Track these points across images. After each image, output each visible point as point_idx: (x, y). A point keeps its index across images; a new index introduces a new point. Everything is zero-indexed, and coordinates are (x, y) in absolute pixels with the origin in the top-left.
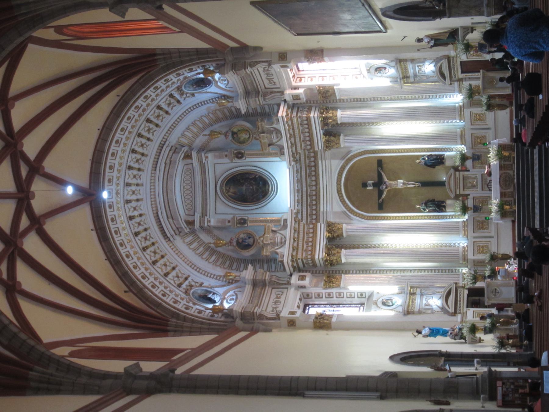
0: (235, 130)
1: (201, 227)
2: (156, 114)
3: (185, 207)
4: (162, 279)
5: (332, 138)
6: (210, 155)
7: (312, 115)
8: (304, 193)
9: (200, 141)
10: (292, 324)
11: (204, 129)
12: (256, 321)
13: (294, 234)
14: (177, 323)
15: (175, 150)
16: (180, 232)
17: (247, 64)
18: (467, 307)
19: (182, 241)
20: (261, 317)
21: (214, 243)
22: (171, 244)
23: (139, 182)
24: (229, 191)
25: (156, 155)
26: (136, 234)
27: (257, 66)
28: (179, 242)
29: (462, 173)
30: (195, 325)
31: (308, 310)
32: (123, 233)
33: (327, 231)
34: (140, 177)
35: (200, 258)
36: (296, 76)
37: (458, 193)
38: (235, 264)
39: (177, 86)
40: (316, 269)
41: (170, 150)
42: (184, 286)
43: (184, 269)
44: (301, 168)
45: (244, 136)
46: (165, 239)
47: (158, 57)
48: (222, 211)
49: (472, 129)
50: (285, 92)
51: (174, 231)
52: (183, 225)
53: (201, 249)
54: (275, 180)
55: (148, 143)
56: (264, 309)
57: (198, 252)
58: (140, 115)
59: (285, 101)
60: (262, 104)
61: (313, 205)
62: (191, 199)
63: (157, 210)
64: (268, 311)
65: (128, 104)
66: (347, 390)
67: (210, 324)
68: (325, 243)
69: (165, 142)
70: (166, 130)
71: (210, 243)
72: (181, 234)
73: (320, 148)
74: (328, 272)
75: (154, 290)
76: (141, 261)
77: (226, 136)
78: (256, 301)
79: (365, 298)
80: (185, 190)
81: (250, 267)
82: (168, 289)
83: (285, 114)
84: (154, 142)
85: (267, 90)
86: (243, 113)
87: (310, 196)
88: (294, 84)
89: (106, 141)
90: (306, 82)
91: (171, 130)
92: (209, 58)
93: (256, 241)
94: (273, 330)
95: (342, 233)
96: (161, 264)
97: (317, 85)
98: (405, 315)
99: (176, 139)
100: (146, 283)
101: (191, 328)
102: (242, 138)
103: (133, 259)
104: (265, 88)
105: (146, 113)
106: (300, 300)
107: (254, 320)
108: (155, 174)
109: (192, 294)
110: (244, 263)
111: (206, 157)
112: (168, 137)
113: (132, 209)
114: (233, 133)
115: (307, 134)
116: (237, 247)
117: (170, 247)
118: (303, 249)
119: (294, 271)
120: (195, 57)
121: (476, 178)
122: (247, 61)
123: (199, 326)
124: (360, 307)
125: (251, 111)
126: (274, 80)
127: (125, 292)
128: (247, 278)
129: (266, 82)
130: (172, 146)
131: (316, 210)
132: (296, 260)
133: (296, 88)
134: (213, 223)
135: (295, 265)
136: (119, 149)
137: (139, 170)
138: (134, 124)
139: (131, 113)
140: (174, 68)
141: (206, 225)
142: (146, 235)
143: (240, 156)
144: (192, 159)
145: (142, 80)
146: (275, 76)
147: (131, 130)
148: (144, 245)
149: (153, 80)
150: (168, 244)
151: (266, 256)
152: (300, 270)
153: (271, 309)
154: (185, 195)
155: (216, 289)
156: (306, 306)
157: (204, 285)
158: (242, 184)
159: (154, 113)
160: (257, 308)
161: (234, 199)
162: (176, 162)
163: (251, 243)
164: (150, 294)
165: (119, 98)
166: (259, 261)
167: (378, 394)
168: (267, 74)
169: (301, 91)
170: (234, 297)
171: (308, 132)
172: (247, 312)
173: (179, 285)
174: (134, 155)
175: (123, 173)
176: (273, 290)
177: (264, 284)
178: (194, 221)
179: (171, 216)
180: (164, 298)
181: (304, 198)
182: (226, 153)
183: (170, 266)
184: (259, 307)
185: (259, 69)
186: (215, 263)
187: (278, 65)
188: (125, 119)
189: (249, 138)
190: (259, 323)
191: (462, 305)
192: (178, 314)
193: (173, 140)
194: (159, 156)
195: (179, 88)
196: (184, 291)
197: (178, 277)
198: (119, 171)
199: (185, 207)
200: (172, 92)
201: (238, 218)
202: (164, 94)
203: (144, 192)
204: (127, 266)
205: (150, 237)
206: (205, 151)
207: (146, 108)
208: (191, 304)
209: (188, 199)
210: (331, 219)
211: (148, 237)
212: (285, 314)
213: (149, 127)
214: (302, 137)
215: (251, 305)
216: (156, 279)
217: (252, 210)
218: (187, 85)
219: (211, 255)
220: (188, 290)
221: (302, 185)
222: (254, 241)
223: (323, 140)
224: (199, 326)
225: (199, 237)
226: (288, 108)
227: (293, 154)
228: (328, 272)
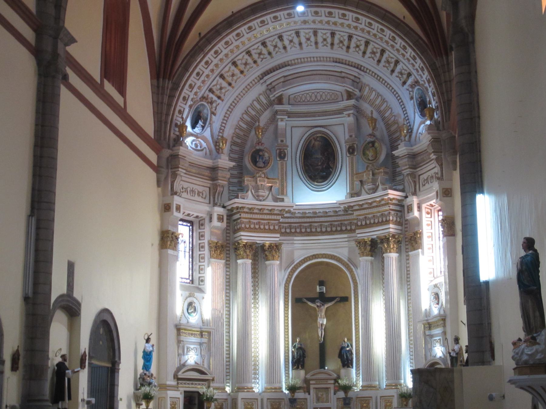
0: (376, 145)
1: (276, 113)
2: (390, 59)
3: (298, 94)
4: (217, 72)
5: (368, 248)
6: (351, 119)
7: (391, 226)
8: (313, 220)
9: (367, 108)
10: (167, 208)
11: (379, 112)
12: (170, 171)
13: (267, 209)
14: (168, 88)
15: (356, 82)
16: (270, 90)
17: (440, 154)
18: (185, 392)
19: (261, 92)
20: (175, 176)
21: (259, 125)
22: (256, 81)
23: (320, 45)
24: (315, 140)
25: (349, 62)
26: (264, 44)
27: (437, 165)
28: (260, 88)
29: (332, 386)
30: (165, 107)
31: (187, 225)
32: (264, 29)
34: (325, 45)
35: (244, 111)
36: (432, 208)
37: (311, 382)
38: (237, 149)
39: (420, 81)
40: (231, 233)
41: (355, 77)
42: (211, 95)
43: (230, 96)
44: (340, 215)
45: (370, 154)
46: (261, 74)
47: (444, 58)
48: (295, 134)
49: (377, 397)
50: (414, 197)
51: (271, 84)
52: (277, 93)
53: (253, 113)
54: (327, 189)
55: (361, 53)
56: (183, 179)
57: (250, 109)
58: (387, 42)
59: (406, 197)
60: (403, 172)
61: (301, 229)
62: (301, 101)
63: (292, 65)
64: (182, 183)
65: (396, 28)
66: (37, 261)
67: (166, 123)
68: (258, 242)
69: (363, 71)
70: (376, 71)
71: (259, 122)
72: (268, 92)
73: (359, 235)
74: (228, 245)
75: (203, 63)
76: (235, 49)
77: (370, 135)
78: (194, 171)
79: (199, 285)
80: (316, 93)
81: (232, 164)
82: (206, 79)
83: (391, 197)
84: (362, 59)
85: (417, 177)
86: (393, 152)
87: (311, 225)
88: (424, 206)
89: (357, 7)
90: (426, 220)
91: (376, 76)
92: (445, 113)
93: (260, 169)
94: (160, 189)
95: (269, 260)
96: (233, 70)
97: (422, 230)
98: (176, 326)
99: (367, 83)
100: (210, 56)
101: (162, 103)
102: (368, 152)
103: (236, 40)
104: (419, 176)
105: (389, 48)
106: (197, 217)
107: (171, 169)
108: (330, 61)
109: (203, 105)
110: (238, 158)
111: (349, 115)
112: (369, 74)
113: (290, 38)
114: (373, 143)
115: (372, 221)
116: (254, 149)
117: (254, 80)
118: (251, 219)
119: (228, 210)
120: (446, 98)
121: (327, 401)
122: (443, 154)
123: (164, 112)
124: (189, 279)
125: (397, 161)
126: (427, 185)
127: (200, 34)
128: (219, 160)
129: (425, 176)
130: (359, 78)
131: (296, 232)
132: (239, 212)
133: (419, 208)
134: (281, 124)
135: (235, 211)
136: (350, 22)
137: (332, 44)
138: (378, 37)
139: (388, 32)
140: (435, 76)
141: (278, 117)
142: (264, 54)
143: (351, 150)
144: (347, 100)
145: (421, 42)
147: (371, 34)
148: (253, 52)
149: (422, 54)
150: (256, 78)
151: (244, 181)
152: (229, 216)
153: (185, 187)
154: (310, 94)
155: (209, 129)
156: (192, 223)
157: (213, 116)
158: (323, 154)
159: (392, 58)
160: (184, 171)
161: (308, 146)
162: (343, 83)
163: (258, 164)
164: (199, 60)
165: (402, 18)
166: (240, 172)
167: (30, 294)
168: (432, 177)
169: (416, 213)
170: (199, 148)
171: (374, 223)
172: (179, 161)
173: (211, 91)
174: (346, 38)
175: (326, 26)
176: (208, 189)
177: (213, 179)
179: (287, 81)
180: (194, 74)
181: (308, 220)
182: (354, 136)
183: (232, 80)
184: (186, 174)
185: (436, 168)
186: (238, 127)
187: (438, 189)
188: (380, 27)
189: (369, 160)
190: (168, 173)
191: (187, 386)
192: (177, 89)
193: (366, 79)
194: (348, 65)
195: (417, 82)
196: (205, 95)
197: (221, 88)
198: (328, 23)
199: (298, 94)
200: (413, 76)
201: (286, 150)
202: (410, 67)
203: (309, 50)
204: (227, 35)
205: (263, 59)
206: (356, 113)
207: (395, 49)
208: (190, 103)
209: (306, 98)
210: (285, 249)
211: (262, 56)
212: (177, 200)
213: (377, 53)
214: (370, 216)
215: (187, 165)
217: (296, 165)
218: (420, 92)
219: (247, 123)
220: (207, 99)
221: (321, 217)
222: (261, 168)
223: (366, 238)
224: (164, 112)
225: (265, 110)
226: (399, 201)
227: (352, 207)
228: (228, 245)
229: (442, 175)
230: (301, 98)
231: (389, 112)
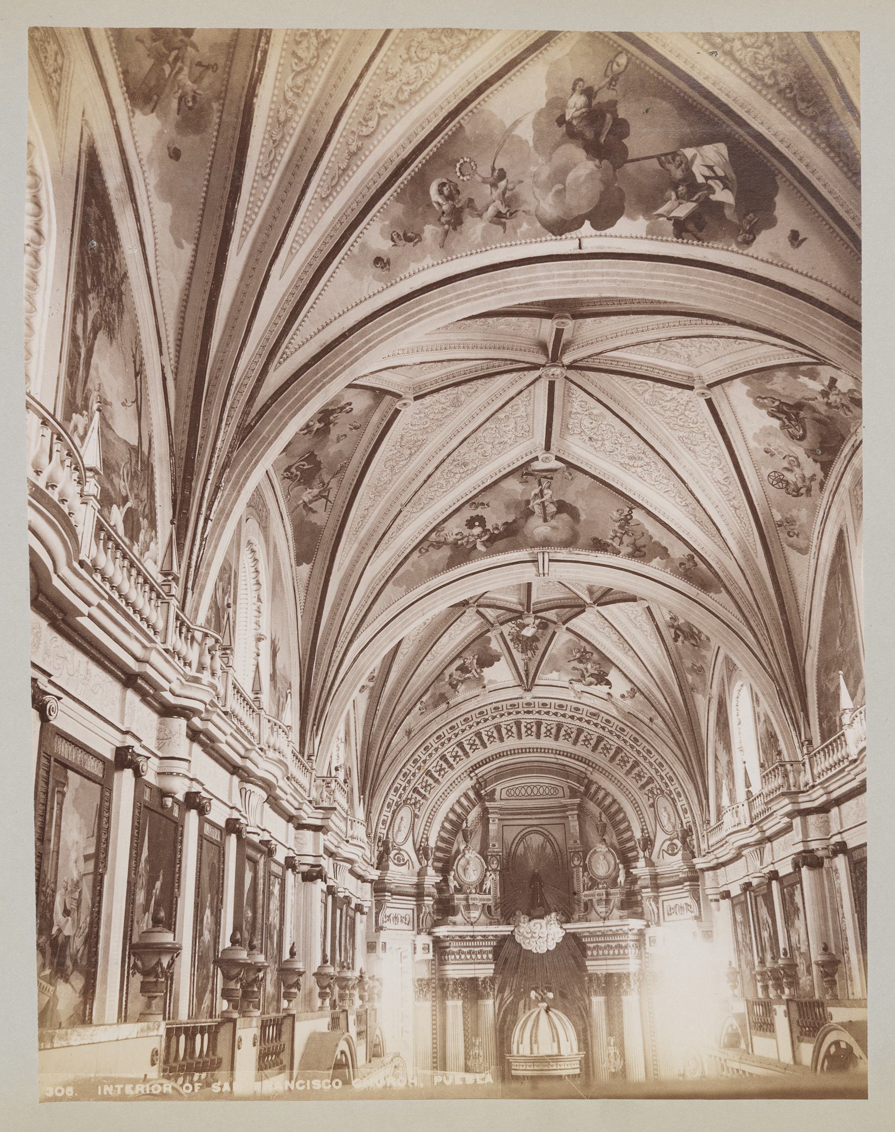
33: (485, 978)
56: (388, 905)
58: (625, 741)
69: (591, 766)
126: (674, 915)
129: (672, 904)
146: (679, 917)
178: (494, 800)
193: (596, 777)
196: (409, 796)
202: (653, 772)
216: (425, 762)
229: (700, 914)
230: (515, 792)
231: (627, 823)
